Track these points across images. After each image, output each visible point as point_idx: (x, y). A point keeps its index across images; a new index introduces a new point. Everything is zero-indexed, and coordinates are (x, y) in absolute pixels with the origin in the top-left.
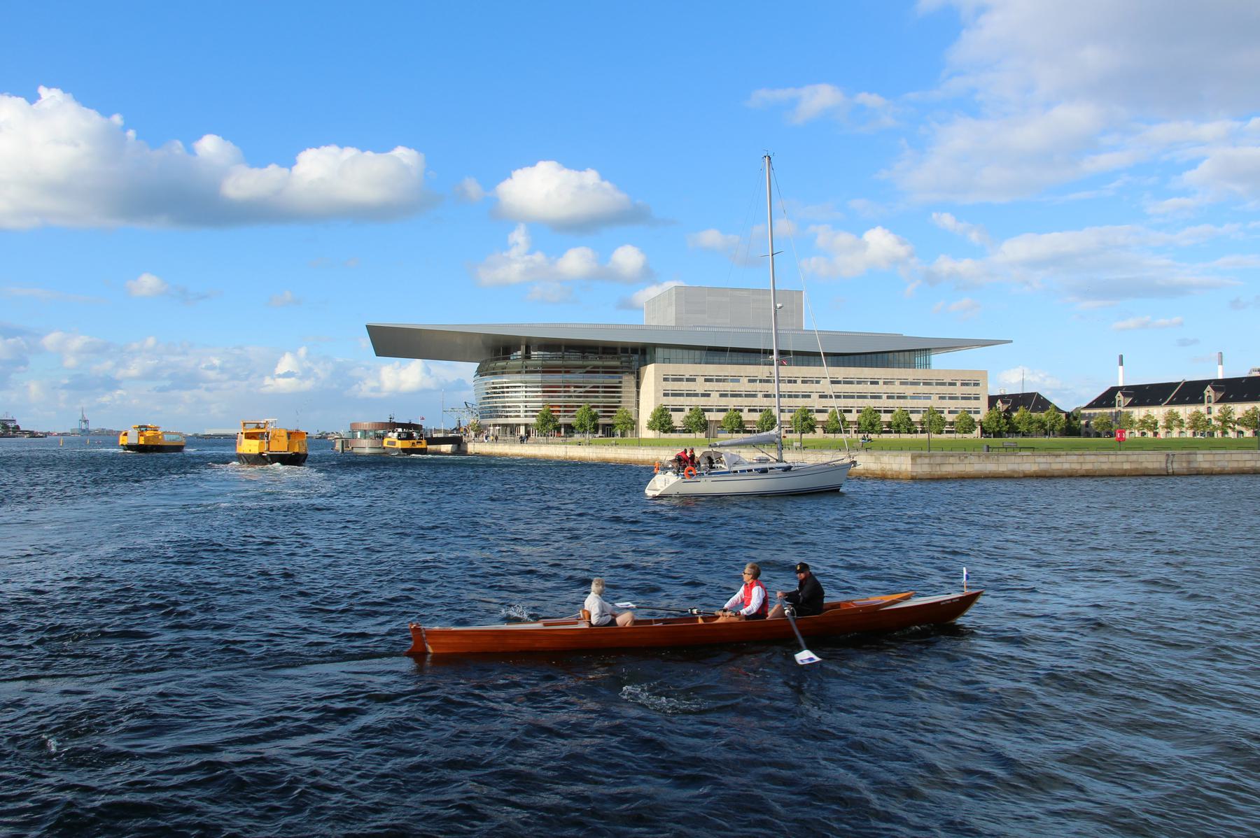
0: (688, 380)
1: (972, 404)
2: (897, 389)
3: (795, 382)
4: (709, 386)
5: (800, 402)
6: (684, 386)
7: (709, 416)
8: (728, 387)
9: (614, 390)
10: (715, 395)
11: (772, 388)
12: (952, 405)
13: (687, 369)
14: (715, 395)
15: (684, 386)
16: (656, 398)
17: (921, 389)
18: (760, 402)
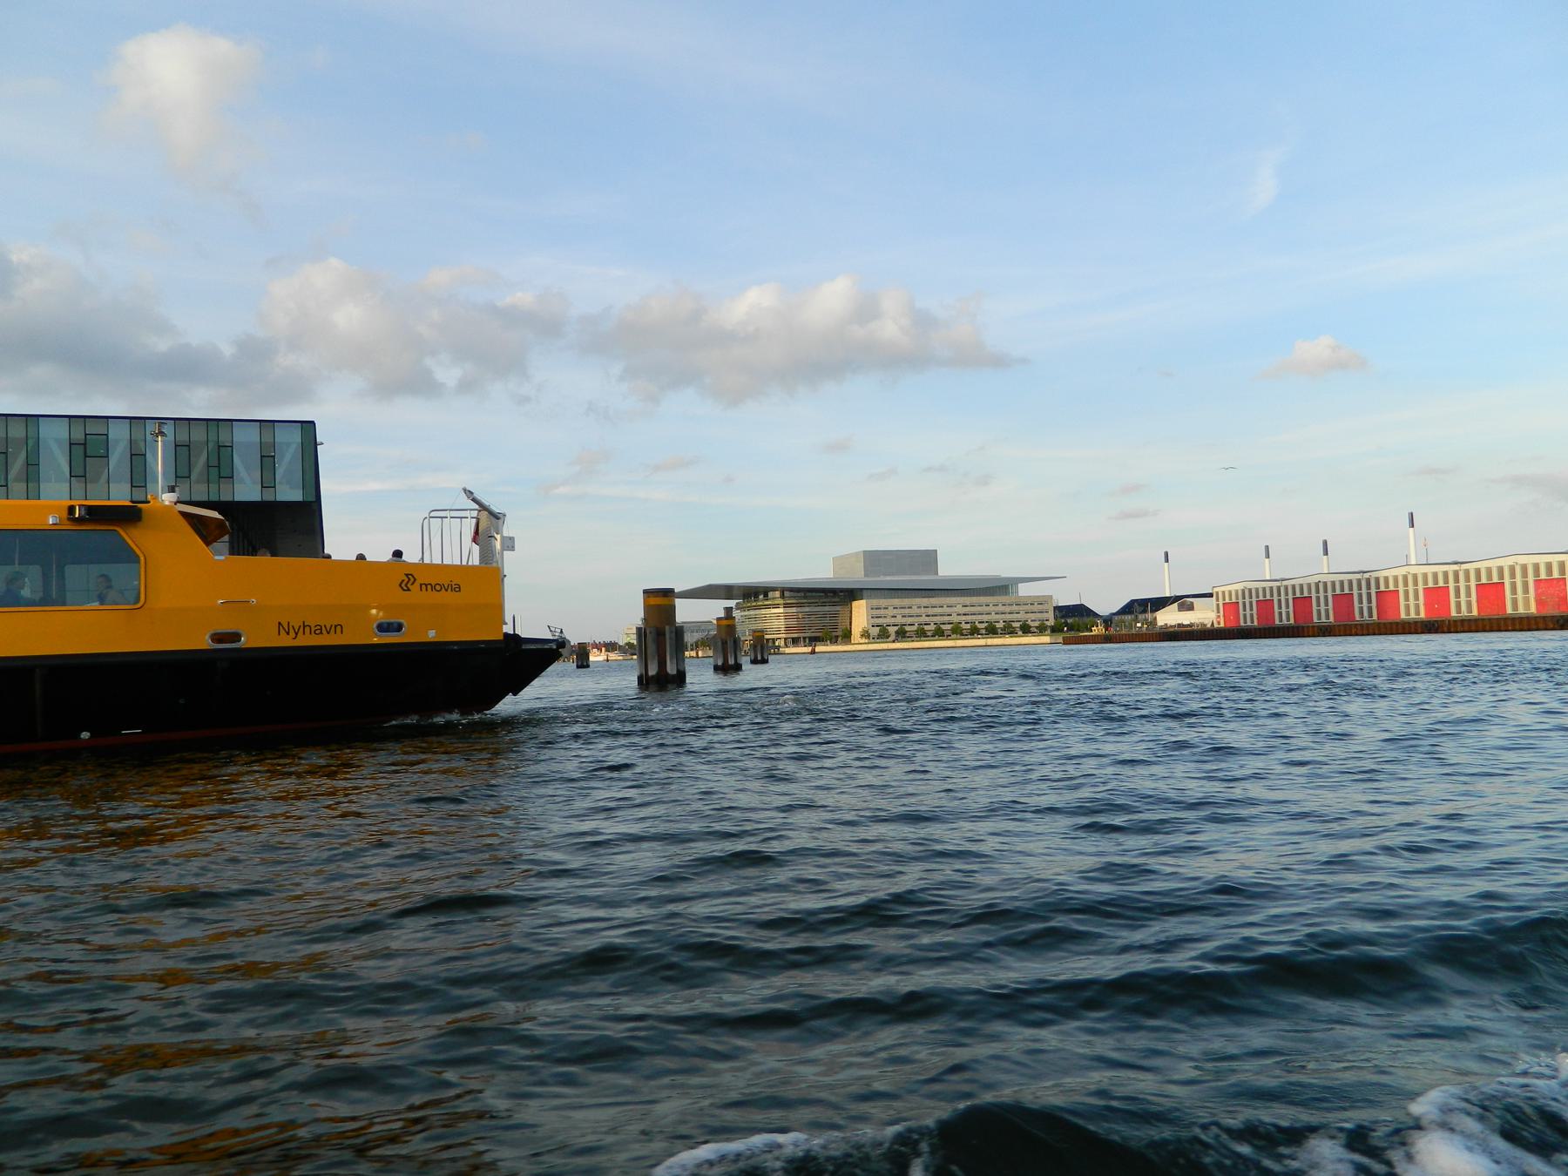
0: (885, 608)
1: (1045, 616)
2: (1001, 608)
3: (942, 607)
4: (895, 611)
5: (946, 619)
6: (882, 612)
7: (907, 628)
8: (907, 611)
9: (835, 616)
10: (899, 617)
11: (930, 611)
12: (1033, 616)
13: (883, 602)
14: (899, 617)
15: (882, 612)
16: (868, 620)
17: (1015, 608)
18: (924, 619)
